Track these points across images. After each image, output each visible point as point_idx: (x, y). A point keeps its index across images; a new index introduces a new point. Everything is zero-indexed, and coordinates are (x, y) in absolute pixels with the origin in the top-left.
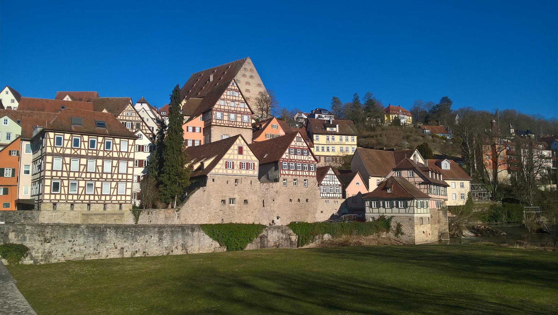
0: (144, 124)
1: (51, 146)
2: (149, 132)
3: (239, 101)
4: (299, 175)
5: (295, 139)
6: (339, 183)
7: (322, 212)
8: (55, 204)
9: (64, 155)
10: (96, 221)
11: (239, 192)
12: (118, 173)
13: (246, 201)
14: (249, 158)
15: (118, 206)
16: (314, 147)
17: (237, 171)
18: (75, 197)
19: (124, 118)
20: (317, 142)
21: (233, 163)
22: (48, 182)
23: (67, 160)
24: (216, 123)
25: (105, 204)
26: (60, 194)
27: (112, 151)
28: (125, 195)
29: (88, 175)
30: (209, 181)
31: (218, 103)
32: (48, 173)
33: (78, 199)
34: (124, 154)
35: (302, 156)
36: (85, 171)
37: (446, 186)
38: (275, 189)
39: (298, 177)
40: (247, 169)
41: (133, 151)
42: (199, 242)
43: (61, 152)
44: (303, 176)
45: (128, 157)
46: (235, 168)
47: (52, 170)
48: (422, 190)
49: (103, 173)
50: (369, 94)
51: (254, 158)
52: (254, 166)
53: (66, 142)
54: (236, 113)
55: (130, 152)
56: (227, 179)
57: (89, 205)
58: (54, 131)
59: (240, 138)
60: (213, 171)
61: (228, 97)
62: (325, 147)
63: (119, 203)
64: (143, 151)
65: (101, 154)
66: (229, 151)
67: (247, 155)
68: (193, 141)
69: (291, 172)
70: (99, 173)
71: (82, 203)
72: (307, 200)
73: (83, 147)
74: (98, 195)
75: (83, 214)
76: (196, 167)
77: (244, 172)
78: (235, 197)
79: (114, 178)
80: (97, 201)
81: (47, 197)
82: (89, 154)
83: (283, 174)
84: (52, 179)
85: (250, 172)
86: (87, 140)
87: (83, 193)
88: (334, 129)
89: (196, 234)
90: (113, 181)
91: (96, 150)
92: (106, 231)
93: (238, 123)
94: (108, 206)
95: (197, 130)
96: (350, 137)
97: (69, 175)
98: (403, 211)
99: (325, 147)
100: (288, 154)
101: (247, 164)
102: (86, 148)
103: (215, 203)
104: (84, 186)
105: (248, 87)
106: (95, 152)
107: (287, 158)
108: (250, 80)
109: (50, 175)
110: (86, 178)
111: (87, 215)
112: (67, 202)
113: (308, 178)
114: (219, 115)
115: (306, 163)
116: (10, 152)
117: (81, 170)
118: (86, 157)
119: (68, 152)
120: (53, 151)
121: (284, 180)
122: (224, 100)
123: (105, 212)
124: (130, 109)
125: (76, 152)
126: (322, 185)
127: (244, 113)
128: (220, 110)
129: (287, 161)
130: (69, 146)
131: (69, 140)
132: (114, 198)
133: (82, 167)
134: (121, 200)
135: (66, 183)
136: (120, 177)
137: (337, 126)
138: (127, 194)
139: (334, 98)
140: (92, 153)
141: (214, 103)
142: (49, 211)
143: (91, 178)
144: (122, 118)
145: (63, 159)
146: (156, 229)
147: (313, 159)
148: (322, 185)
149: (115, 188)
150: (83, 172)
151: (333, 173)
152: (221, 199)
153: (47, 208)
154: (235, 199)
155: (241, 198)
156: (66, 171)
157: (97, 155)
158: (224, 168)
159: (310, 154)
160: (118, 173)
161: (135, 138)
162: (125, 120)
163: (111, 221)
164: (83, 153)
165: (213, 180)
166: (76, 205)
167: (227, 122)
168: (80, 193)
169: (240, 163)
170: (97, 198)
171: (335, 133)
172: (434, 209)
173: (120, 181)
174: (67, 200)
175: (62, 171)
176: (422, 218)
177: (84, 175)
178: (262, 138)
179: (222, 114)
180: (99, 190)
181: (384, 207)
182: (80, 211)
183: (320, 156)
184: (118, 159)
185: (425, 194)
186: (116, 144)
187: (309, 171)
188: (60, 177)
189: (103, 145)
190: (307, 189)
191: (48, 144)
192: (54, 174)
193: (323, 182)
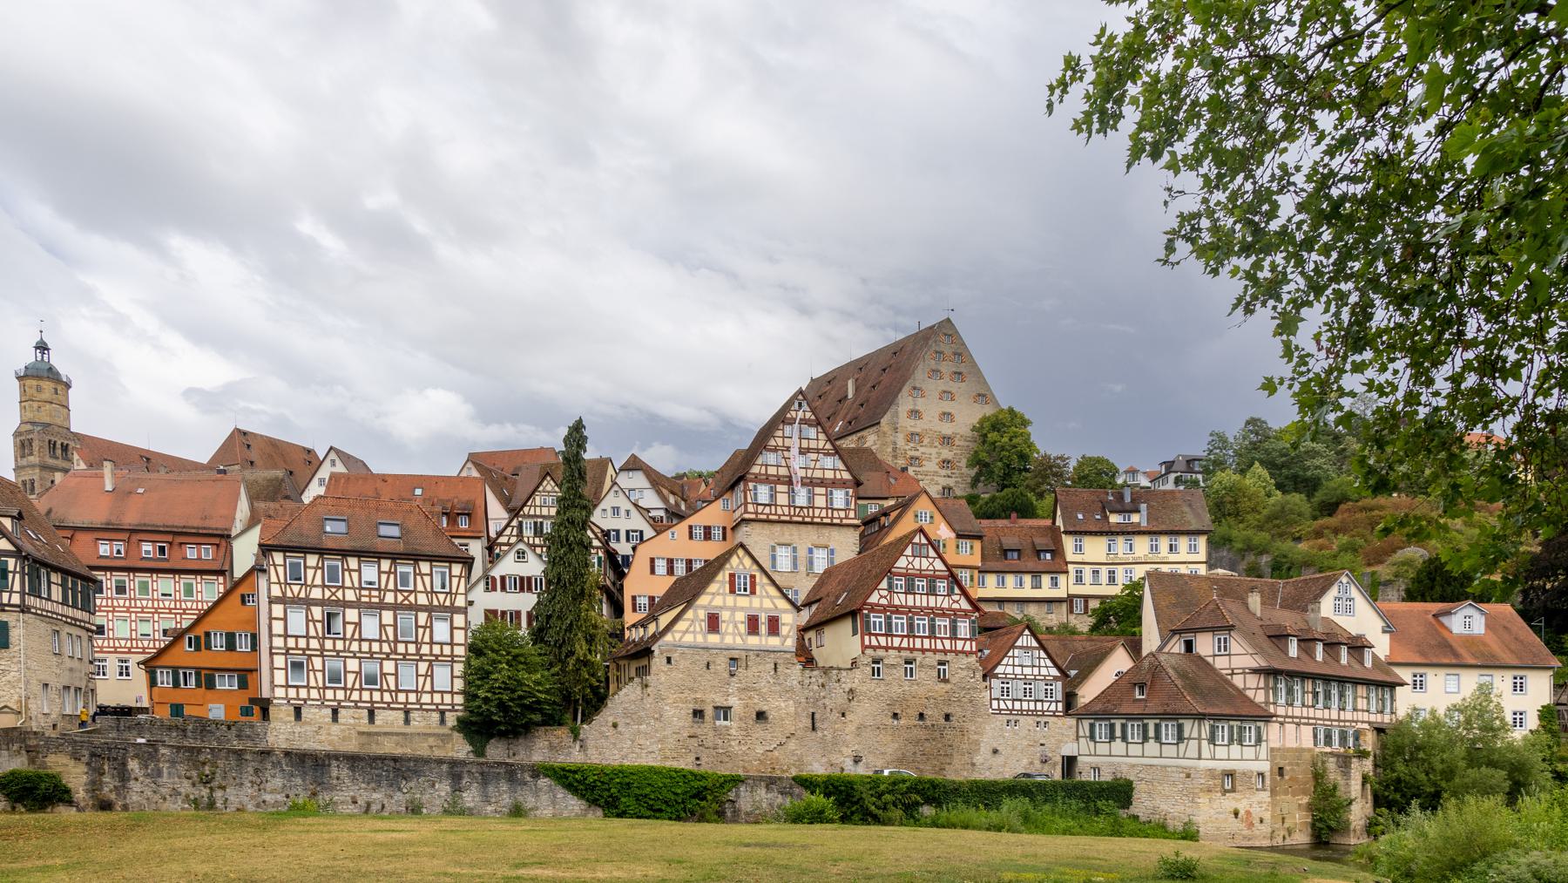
3: (817, 451)
4: (923, 651)
5: (908, 551)
7: (995, 751)
12: (432, 643)
13: (761, 716)
14: (767, 604)
20: (1079, 558)
27: (415, 591)
29: (365, 646)
30: (658, 662)
34: (442, 597)
35: (932, 599)
37: (1392, 686)
39: (919, 656)
42: (554, 803)
43: (302, 595)
44: (935, 651)
54: (810, 483)
56: (706, 657)
58: (284, 549)
60: (668, 638)
62: (1104, 571)
65: (389, 598)
67: (762, 597)
68: (689, 562)
69: (896, 642)
72: (947, 717)
73: (348, 583)
78: (730, 703)
83: (870, 647)
91: (379, 589)
93: (817, 512)
95: (717, 533)
96: (1183, 543)
99: (1104, 571)
100: (884, 593)
103: (677, 716)
105: (947, 406)
106: (375, 593)
107: (884, 602)
108: (954, 387)
113: (949, 657)
114: (763, 493)
115: (944, 615)
116: (243, 597)
117: (349, 635)
119: (316, 594)
123: (408, 730)
127: (835, 484)
128: (767, 479)
129: (884, 611)
130: (318, 581)
131: (316, 568)
133: (350, 628)
136: (437, 649)
143: (370, 652)
145: (308, 610)
146: (445, 767)
147: (965, 605)
150: (352, 639)
151: (1035, 644)
159: (957, 590)
165: (669, 660)
167: (786, 510)
171: (1130, 532)
183: (1086, 598)
184: (429, 609)
186: (422, 575)
190: (948, 686)
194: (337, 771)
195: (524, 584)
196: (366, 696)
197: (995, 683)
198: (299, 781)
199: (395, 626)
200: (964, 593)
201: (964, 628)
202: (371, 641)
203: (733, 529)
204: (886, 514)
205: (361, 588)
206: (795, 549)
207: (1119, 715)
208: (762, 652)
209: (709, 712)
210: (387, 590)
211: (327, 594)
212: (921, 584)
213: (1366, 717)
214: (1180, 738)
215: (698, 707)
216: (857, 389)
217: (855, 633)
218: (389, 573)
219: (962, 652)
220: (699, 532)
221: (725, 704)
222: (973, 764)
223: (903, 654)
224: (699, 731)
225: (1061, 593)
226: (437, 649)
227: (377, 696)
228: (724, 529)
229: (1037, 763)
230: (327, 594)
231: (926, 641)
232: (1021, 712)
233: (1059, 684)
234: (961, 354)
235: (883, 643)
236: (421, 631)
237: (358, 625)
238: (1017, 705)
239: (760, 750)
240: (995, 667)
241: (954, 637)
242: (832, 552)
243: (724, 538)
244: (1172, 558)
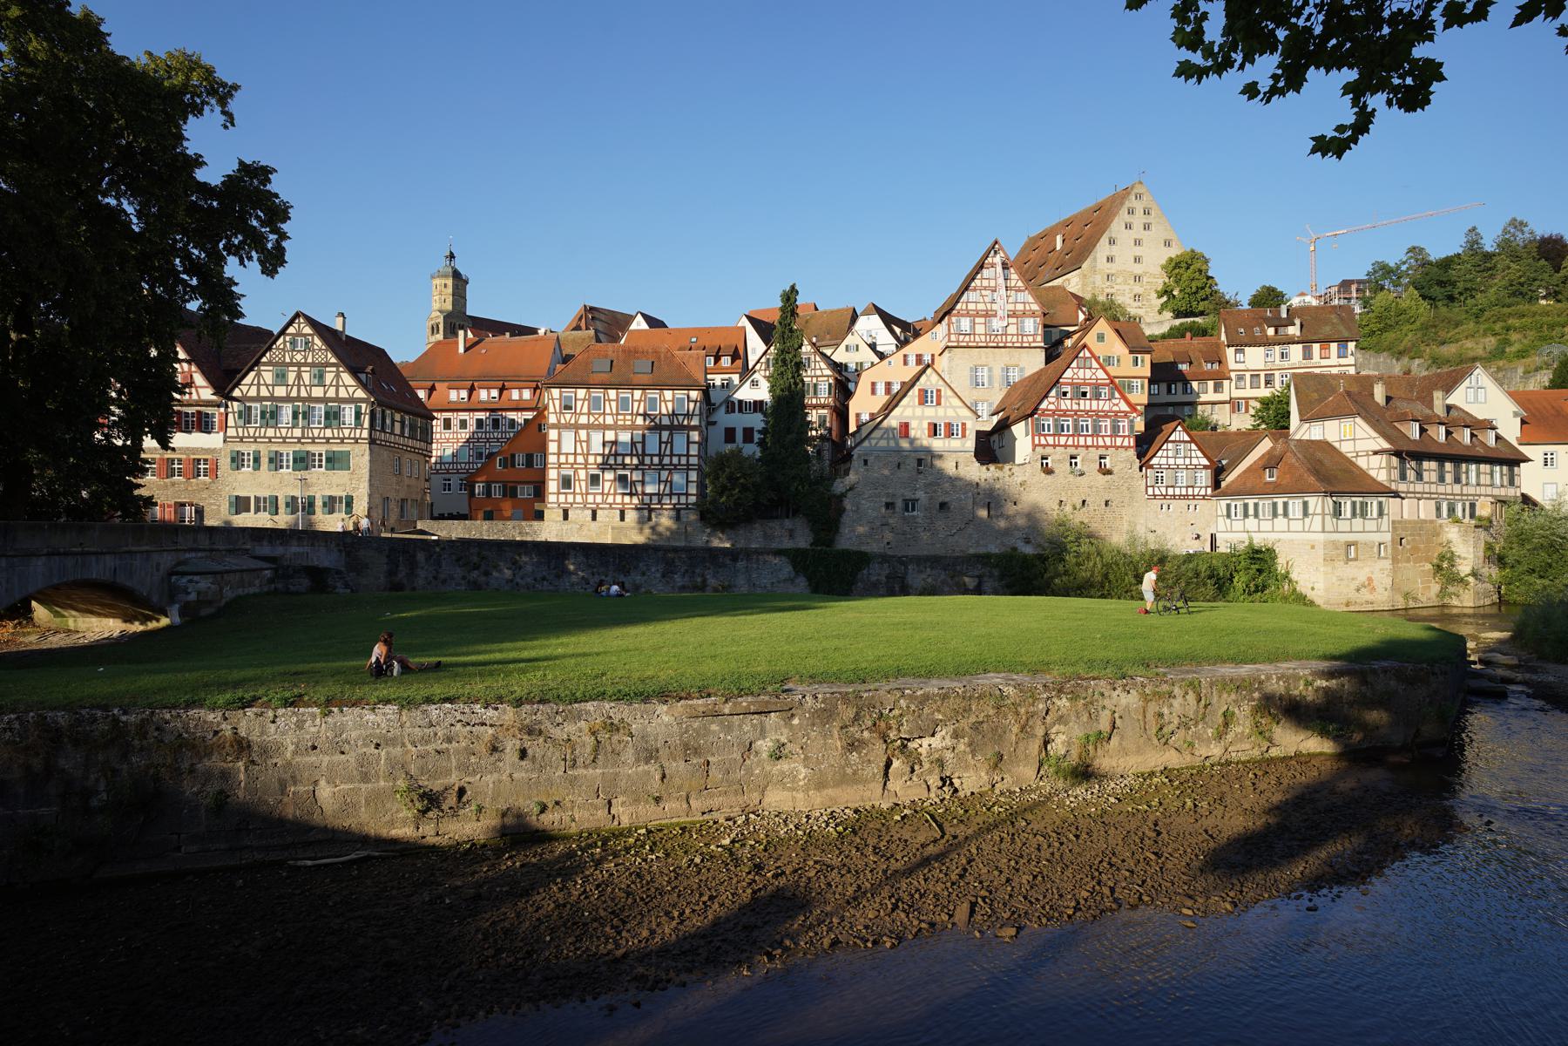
5: (1074, 365)
9: (577, 427)
11: (926, 486)
12: (672, 455)
14: (950, 413)
18: (599, 499)
20: (1241, 366)
23: (583, 434)
26: (574, 493)
28: (687, 494)
31: (964, 298)
32: (552, 459)
33: (604, 502)
39: (1082, 451)
44: (1098, 447)
47: (559, 454)
49: (644, 454)
52: (964, 430)
53: (579, 403)
60: (866, 444)
61: (985, 283)
69: (1063, 440)
85: (955, 443)
101: (949, 426)
105: (1138, 251)
107: (1052, 407)
108: (1144, 235)
114: (965, 324)
115: (1106, 416)
119: (583, 420)
126: (1151, 467)
128: (968, 315)
130: (585, 410)
136: (675, 460)
147: (1124, 407)
148: (1151, 467)
151: (1187, 438)
155: (931, 498)
160: (672, 455)
164: (609, 420)
165: (866, 462)
166: (599, 512)
174: (585, 503)
175: (575, 454)
192: (563, 459)
193: (1154, 461)
202: (624, 455)
206: (990, 370)
209: (899, 504)
213: (1489, 490)
214: (1306, 514)
225: (1224, 396)
226: (675, 460)
232: (1174, 497)
238: (1170, 491)
242: (1022, 370)
244: (1325, 362)
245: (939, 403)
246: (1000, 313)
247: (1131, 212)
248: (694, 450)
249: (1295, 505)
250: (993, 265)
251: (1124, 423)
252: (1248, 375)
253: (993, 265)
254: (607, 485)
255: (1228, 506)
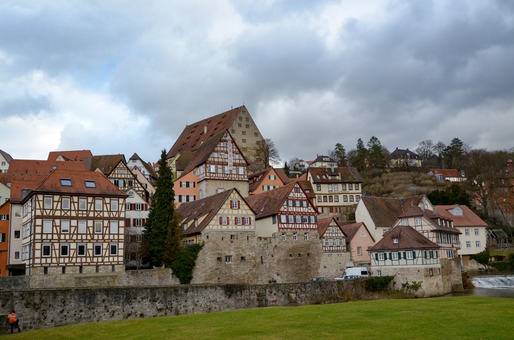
0: (136, 182)
1: (40, 209)
2: (141, 189)
4: (299, 229)
5: (293, 191)
6: (343, 235)
7: (325, 267)
8: (46, 269)
9: (54, 218)
10: (89, 284)
11: (235, 248)
12: (109, 234)
13: (243, 258)
14: (244, 212)
15: (110, 267)
16: (315, 198)
17: (232, 227)
18: (67, 260)
19: (116, 177)
21: (228, 218)
22: (38, 246)
23: (57, 222)
24: (210, 176)
25: (97, 266)
26: (51, 258)
29: (79, 237)
36: (76, 232)
37: (458, 234)
38: (273, 245)
39: (298, 231)
40: (243, 224)
41: (123, 210)
43: (51, 214)
44: (304, 229)
45: (119, 216)
46: (231, 223)
47: (42, 234)
48: (431, 239)
50: (374, 139)
51: (250, 212)
55: (121, 212)
56: (222, 236)
57: (81, 267)
59: (234, 192)
60: (207, 228)
61: (222, 149)
63: (111, 264)
64: (134, 209)
65: (91, 214)
66: (224, 206)
68: (188, 197)
69: (290, 225)
70: (90, 234)
71: (74, 266)
72: (308, 255)
73: (73, 208)
74: (90, 257)
75: (76, 278)
76: (190, 223)
77: (240, 228)
78: (231, 254)
79: (105, 238)
80: (89, 263)
81: (37, 261)
82: (80, 215)
84: (42, 242)
86: (77, 201)
87: (75, 256)
88: (337, 178)
89: (189, 294)
90: (104, 242)
91: (87, 211)
92: (97, 294)
93: (233, 176)
94: (101, 267)
95: (191, 185)
97: (59, 238)
98: (411, 262)
102: (77, 209)
104: (75, 248)
105: (244, 137)
106: (85, 212)
107: (285, 210)
109: (40, 238)
110: (77, 239)
111: (80, 278)
112: (58, 266)
113: (309, 231)
114: (213, 168)
115: (306, 215)
117: (72, 232)
118: (77, 218)
119: (58, 213)
120: (42, 214)
121: (283, 234)
122: (217, 152)
124: (121, 166)
125: (66, 213)
126: (324, 238)
129: (285, 214)
131: (58, 202)
132: (106, 260)
133: (73, 229)
134: (114, 262)
135: (57, 246)
136: (111, 237)
137: (339, 174)
138: (119, 255)
139: (338, 145)
140: (83, 214)
141: (208, 156)
142: (40, 275)
143: (82, 240)
144: (114, 176)
145: (53, 221)
147: (313, 211)
148: (324, 238)
149: (106, 249)
150: (73, 234)
151: (336, 225)
152: (217, 256)
153: (38, 272)
154: (231, 256)
155: (237, 255)
156: (57, 234)
157: (88, 216)
158: (219, 224)
159: (310, 205)
160: (109, 234)
161: (125, 197)
162: (118, 178)
163: (104, 284)
164: (74, 214)
165: (208, 237)
166: (67, 269)
167: (221, 175)
168: (71, 256)
169: (236, 218)
170: (89, 260)
171: (337, 182)
172: (445, 259)
173: (111, 242)
174: (58, 263)
175: (52, 234)
176: (431, 269)
177: (75, 237)
178: (258, 191)
179: (216, 167)
180: (91, 252)
181: (391, 258)
182: (72, 275)
183: (322, 207)
184: (109, 219)
185: (434, 244)
187: (310, 223)
188: (50, 240)
189: (93, 205)
191: (38, 207)
192: (44, 237)
193: (325, 235)
194: (99, 297)
195: (133, 207)
196: (79, 260)
197: (324, 240)
198: (82, 304)
199: (93, 227)
200: (312, 206)
201: (312, 218)
202: (82, 234)
203: (198, 183)
204: (257, 176)
205: (79, 210)
207: (388, 250)
208: (243, 232)
209: (224, 258)
210: (90, 211)
211: (63, 213)
212: (298, 203)
215: (219, 257)
216: (208, 130)
217: (274, 223)
218: (91, 203)
219: (313, 229)
220: (184, 183)
221: (229, 255)
222: (318, 273)
223: (294, 230)
224: (220, 267)
227: (84, 260)
228: (194, 183)
229: (339, 270)
230: (63, 213)
231: (300, 225)
232: (333, 251)
233: (344, 239)
234: (249, 118)
235: (286, 227)
236: (105, 229)
237: (77, 227)
239: (243, 273)
240: (323, 234)
241: (310, 223)
243: (194, 186)
245: (239, 208)
246: (229, 164)
247: (241, 119)
248: (122, 231)
249: (409, 254)
250: (226, 141)
251: (312, 218)
252: (322, 196)
253: (226, 141)
254: (72, 252)
255: (376, 255)
